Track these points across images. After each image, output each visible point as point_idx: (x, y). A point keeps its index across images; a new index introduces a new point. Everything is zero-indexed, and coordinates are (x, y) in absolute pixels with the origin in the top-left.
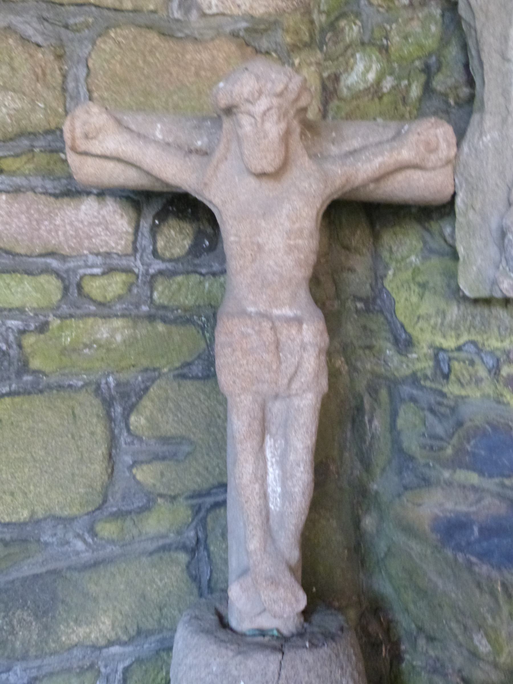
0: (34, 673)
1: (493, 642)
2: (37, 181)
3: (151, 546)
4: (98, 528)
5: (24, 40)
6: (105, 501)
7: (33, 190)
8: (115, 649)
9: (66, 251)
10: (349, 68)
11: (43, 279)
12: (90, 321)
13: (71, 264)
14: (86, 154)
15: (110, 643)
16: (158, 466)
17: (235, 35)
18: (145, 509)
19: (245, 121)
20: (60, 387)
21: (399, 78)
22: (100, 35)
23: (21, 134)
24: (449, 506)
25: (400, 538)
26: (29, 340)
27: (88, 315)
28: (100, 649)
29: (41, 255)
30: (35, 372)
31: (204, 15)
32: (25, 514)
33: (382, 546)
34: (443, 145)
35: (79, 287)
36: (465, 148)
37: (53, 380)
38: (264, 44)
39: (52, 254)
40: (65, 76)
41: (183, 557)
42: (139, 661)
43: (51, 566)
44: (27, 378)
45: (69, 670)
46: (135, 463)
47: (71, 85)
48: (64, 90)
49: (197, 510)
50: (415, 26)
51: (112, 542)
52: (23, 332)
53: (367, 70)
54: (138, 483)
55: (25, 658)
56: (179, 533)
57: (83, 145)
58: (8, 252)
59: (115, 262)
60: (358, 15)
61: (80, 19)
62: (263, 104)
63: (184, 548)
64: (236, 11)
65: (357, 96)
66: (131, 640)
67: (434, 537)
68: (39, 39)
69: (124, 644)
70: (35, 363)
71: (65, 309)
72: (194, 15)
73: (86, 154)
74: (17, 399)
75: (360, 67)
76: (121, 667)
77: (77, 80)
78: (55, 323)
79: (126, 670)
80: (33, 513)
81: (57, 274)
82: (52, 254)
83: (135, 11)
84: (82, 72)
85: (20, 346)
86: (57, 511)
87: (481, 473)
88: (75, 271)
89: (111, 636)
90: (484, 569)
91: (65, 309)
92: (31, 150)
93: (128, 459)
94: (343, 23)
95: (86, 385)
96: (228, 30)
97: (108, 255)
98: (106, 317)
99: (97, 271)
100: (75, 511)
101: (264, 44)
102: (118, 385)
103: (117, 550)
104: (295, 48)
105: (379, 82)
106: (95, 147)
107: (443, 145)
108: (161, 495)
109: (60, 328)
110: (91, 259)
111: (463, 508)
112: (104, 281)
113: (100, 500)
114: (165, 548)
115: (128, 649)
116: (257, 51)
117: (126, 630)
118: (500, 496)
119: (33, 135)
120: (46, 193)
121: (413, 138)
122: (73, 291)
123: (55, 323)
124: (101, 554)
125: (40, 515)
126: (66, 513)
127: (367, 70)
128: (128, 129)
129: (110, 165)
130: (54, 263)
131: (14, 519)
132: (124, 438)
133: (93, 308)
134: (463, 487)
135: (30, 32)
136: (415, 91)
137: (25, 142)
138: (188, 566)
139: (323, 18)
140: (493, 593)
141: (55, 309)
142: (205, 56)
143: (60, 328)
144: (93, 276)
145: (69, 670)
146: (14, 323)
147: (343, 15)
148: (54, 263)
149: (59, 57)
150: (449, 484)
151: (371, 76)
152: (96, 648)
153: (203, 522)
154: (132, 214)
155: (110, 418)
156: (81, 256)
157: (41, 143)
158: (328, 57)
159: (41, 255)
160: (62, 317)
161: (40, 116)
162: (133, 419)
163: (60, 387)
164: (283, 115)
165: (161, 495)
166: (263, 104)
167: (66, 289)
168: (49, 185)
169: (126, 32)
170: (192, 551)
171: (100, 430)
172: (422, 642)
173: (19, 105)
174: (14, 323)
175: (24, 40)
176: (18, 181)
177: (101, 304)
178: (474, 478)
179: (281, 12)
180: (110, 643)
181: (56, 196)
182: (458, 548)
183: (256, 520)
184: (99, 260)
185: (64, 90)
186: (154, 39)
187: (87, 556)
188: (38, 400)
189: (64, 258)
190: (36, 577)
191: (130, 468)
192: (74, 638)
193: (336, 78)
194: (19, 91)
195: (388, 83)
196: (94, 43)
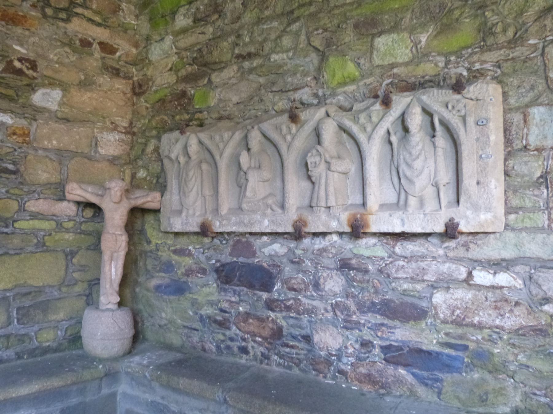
0: (41, 327)
1: (166, 314)
2: (51, 196)
3: (76, 294)
4: (62, 289)
5: (51, 159)
6: (64, 282)
7: (50, 198)
8: (64, 322)
9: (58, 215)
10: (139, 172)
11: (51, 222)
12: (64, 233)
13: (59, 218)
14: (71, 194)
15: (63, 320)
16: (79, 273)
17: (108, 160)
18: (75, 284)
19: (113, 192)
20: (54, 250)
21: (151, 177)
22: (72, 159)
23: (48, 184)
24: (158, 282)
25: (145, 292)
26: (46, 238)
27: (63, 232)
28: (60, 322)
29: (51, 216)
30: (47, 246)
31: (100, 155)
32: (41, 284)
33: (141, 295)
34: (158, 197)
35: (61, 224)
36: (163, 198)
37: (52, 248)
38: (116, 163)
39: (54, 215)
40: (61, 170)
41: (85, 298)
42: (70, 326)
43: (48, 298)
44: (45, 248)
45: (50, 327)
46: (73, 272)
47: (62, 171)
48: (61, 173)
49: (90, 285)
50: (155, 166)
51: (65, 293)
52: (44, 236)
53: (143, 174)
54: (73, 277)
55: (38, 323)
56: (84, 291)
57: (70, 192)
58: (42, 214)
59: (71, 218)
60: (142, 159)
61: (66, 155)
62: (116, 189)
63: (85, 295)
64: (109, 154)
65: (140, 179)
66: (69, 320)
67: (154, 291)
68: (55, 159)
69: (66, 321)
70: (47, 244)
71: (57, 230)
72: (97, 155)
73: (71, 194)
74: (42, 253)
75: (142, 172)
76: (65, 327)
77: (64, 170)
78: (54, 233)
79: (67, 328)
80: (44, 284)
81: (55, 221)
82: (54, 215)
83: (82, 153)
84: (66, 168)
85: (43, 239)
86: (50, 284)
87: (165, 273)
88: (60, 220)
89: (63, 318)
90: (165, 297)
91: (57, 230)
92: (50, 188)
93: (71, 271)
94: (138, 160)
95: (61, 250)
96: (107, 159)
97: (70, 216)
98: (68, 232)
99: (66, 220)
100: (56, 284)
101: (116, 163)
102: (70, 251)
103: (66, 295)
104: (125, 164)
105: (146, 177)
106: (74, 192)
107: (158, 197)
108: (80, 281)
109: (55, 235)
110: (65, 217)
111: (160, 282)
112: (68, 223)
113: (62, 281)
114: (80, 295)
115: (67, 322)
116: (114, 164)
117: (67, 317)
118: (169, 278)
119: (51, 184)
120: (53, 199)
121: (151, 196)
122: (59, 226)
123: (54, 233)
124: (62, 296)
125: (45, 285)
126: (53, 284)
127: (143, 174)
128: (82, 189)
129: (77, 196)
130: (55, 218)
131: (38, 285)
132: (70, 265)
133: (64, 230)
134: (161, 277)
135: (52, 157)
136: (154, 181)
137: (49, 186)
138: (86, 300)
139: (133, 157)
140: (166, 302)
141: (54, 230)
142: (100, 166)
143: (55, 235)
144: (65, 222)
145: (50, 327)
146: (42, 233)
147: (139, 158)
148: (55, 218)
149: (60, 164)
150: (158, 277)
151: (144, 175)
152: (58, 322)
153: (91, 289)
154: (77, 205)
155: (67, 260)
156: (62, 216)
157: (53, 186)
158: (133, 168)
159: (51, 216)
160: (56, 232)
161: (54, 179)
162: (73, 260)
163: (54, 250)
164: (121, 191)
165: (80, 281)
166: (116, 189)
167: (57, 225)
168: (55, 197)
169: (79, 158)
170: (87, 296)
171: (64, 263)
172: (150, 319)
173: (48, 176)
174: (42, 233)
175: (51, 159)
176: (46, 196)
177: (67, 229)
178: (163, 274)
179: (121, 155)
180: (63, 320)
181: (56, 200)
182: (160, 292)
183: (109, 280)
184: (67, 218)
185: (61, 173)
186: (86, 160)
187: (58, 296)
188: (47, 254)
189: (57, 217)
190: (44, 301)
191: (72, 273)
192: (53, 318)
193: (135, 173)
194: (49, 173)
195: (148, 178)
196: (70, 161)
